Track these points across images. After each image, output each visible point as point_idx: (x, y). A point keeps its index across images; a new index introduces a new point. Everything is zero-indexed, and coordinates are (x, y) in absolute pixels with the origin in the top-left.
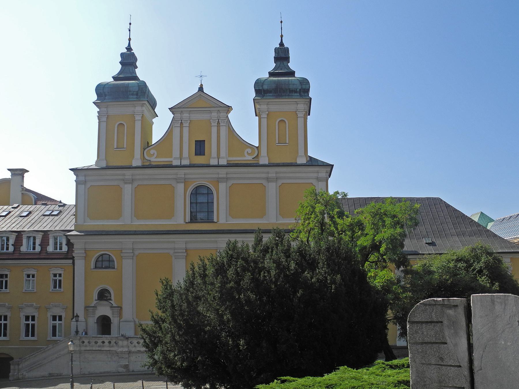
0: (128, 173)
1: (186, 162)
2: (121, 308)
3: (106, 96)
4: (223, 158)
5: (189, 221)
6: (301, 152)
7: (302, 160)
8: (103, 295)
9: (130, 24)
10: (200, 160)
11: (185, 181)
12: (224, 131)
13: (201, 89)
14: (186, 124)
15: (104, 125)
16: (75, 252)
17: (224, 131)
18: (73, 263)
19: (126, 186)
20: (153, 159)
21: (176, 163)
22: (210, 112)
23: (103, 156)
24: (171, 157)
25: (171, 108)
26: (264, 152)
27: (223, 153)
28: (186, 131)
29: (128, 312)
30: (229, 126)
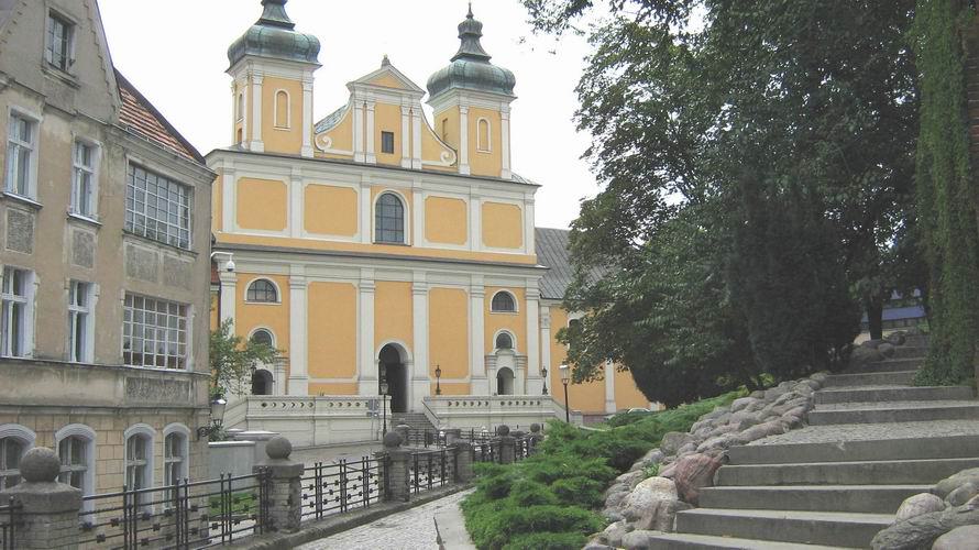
1: (371, 160)
4: (418, 160)
6: (505, 165)
7: (505, 176)
10: (388, 159)
11: (372, 187)
12: (417, 122)
13: (386, 62)
17: (417, 122)
18: (219, 293)
19: (294, 183)
20: (327, 149)
21: (359, 159)
22: (401, 95)
24: (351, 150)
27: (417, 154)
28: (370, 115)
29: (298, 365)
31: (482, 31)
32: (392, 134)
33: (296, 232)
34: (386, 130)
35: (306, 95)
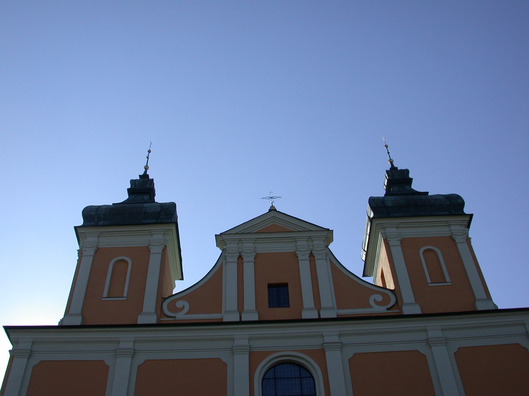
6: (479, 293)
9: (149, 151)
15: (88, 262)
23: (78, 308)
25: (221, 234)
26: (408, 296)
28: (249, 269)
30: (331, 261)
31: (411, 176)
32: (286, 285)
34: (272, 282)
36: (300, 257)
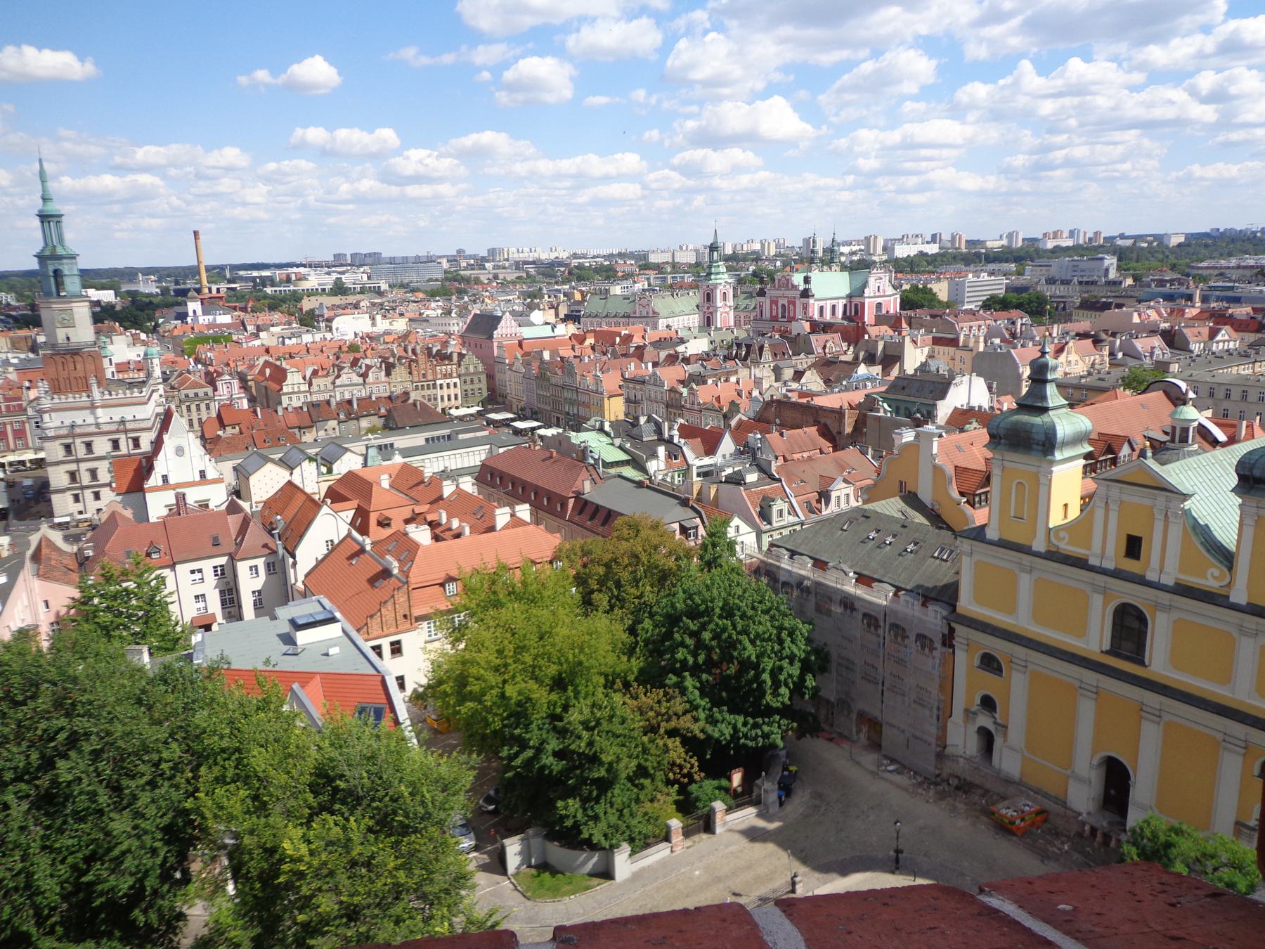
0: (1026, 559)
1: (1109, 565)
2: (1006, 727)
3: (1001, 438)
5: (1108, 648)
8: (988, 703)
10: (1131, 566)
11: (1104, 591)
14: (1113, 507)
16: (957, 639)
21: (1093, 561)
24: (1089, 549)
28: (1113, 517)
33: (1022, 621)
35: (1043, 490)
36: (1157, 516)
